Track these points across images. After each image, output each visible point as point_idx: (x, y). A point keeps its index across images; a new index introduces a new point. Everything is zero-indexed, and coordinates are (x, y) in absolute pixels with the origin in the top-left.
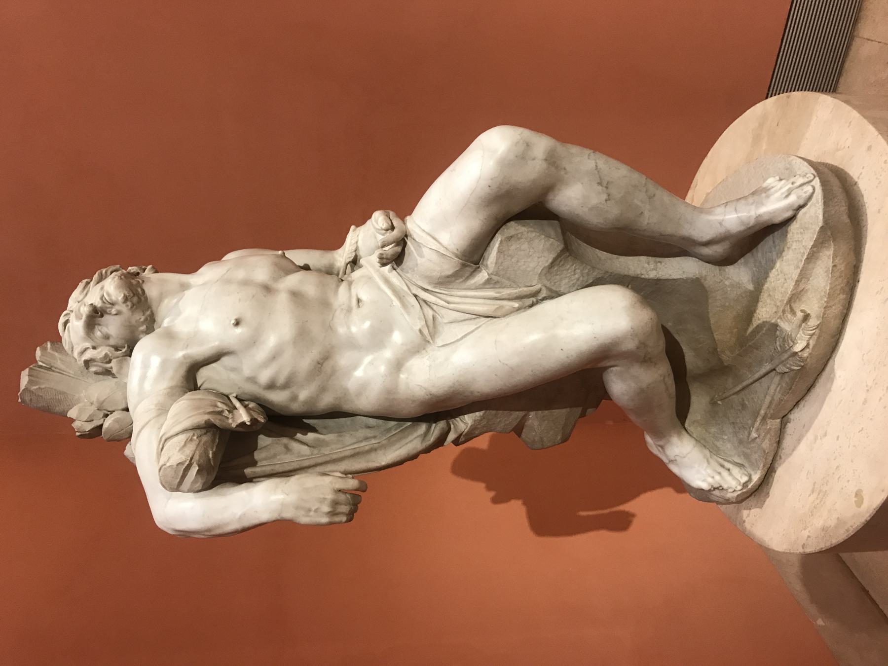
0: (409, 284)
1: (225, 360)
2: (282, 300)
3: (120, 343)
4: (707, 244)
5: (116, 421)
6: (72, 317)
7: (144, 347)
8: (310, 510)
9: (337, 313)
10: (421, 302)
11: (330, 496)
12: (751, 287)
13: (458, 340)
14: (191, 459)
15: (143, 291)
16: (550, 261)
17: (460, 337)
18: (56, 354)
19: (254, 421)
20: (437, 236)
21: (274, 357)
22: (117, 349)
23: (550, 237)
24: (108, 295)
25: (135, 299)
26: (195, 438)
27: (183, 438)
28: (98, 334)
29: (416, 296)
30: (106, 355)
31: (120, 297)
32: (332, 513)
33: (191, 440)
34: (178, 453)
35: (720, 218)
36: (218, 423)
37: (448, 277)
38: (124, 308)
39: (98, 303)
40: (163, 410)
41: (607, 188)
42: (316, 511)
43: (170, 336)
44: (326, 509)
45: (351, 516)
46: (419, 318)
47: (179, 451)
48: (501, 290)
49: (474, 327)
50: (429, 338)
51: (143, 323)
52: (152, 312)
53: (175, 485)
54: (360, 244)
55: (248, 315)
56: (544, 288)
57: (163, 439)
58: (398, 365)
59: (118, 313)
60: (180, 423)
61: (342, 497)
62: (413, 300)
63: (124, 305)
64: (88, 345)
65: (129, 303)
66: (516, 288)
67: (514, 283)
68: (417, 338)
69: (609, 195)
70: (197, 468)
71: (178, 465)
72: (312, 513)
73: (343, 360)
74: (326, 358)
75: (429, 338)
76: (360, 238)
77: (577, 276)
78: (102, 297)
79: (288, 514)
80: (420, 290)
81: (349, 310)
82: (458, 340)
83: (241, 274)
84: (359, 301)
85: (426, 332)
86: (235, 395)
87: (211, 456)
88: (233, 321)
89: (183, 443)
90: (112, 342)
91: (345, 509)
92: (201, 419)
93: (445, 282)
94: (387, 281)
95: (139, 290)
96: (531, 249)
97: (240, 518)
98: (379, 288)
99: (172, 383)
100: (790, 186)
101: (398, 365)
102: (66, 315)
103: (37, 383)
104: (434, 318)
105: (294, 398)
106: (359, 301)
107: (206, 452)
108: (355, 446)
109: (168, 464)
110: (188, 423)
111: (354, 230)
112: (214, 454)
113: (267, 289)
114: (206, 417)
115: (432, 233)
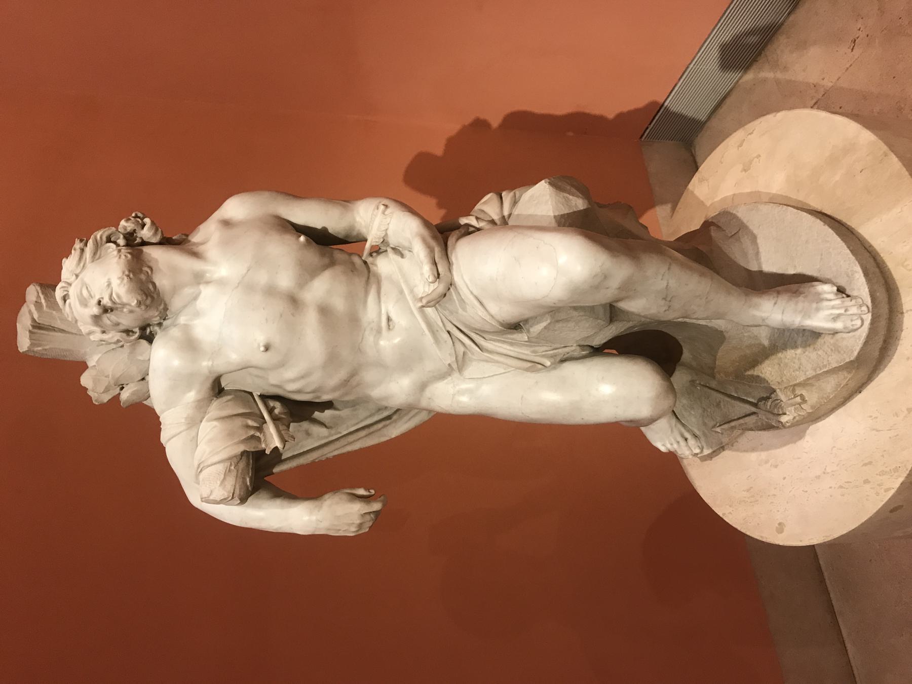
2: (311, 320)
9: (367, 333)
15: (154, 284)
23: (597, 318)
24: (119, 297)
25: (148, 302)
26: (232, 468)
29: (449, 332)
31: (134, 303)
33: (230, 471)
35: (764, 315)
40: (193, 423)
43: (190, 345)
55: (276, 340)
58: (423, 386)
60: (217, 453)
61: (368, 517)
62: (446, 336)
65: (143, 307)
69: (669, 307)
73: (369, 376)
74: (353, 374)
76: (391, 226)
80: (455, 329)
81: (379, 331)
84: (389, 319)
88: (262, 349)
90: (122, 327)
95: (151, 287)
99: (200, 397)
100: (842, 311)
103: (39, 345)
104: (464, 353)
106: (389, 319)
107: (244, 479)
110: (224, 455)
114: (242, 448)
115: (480, 297)
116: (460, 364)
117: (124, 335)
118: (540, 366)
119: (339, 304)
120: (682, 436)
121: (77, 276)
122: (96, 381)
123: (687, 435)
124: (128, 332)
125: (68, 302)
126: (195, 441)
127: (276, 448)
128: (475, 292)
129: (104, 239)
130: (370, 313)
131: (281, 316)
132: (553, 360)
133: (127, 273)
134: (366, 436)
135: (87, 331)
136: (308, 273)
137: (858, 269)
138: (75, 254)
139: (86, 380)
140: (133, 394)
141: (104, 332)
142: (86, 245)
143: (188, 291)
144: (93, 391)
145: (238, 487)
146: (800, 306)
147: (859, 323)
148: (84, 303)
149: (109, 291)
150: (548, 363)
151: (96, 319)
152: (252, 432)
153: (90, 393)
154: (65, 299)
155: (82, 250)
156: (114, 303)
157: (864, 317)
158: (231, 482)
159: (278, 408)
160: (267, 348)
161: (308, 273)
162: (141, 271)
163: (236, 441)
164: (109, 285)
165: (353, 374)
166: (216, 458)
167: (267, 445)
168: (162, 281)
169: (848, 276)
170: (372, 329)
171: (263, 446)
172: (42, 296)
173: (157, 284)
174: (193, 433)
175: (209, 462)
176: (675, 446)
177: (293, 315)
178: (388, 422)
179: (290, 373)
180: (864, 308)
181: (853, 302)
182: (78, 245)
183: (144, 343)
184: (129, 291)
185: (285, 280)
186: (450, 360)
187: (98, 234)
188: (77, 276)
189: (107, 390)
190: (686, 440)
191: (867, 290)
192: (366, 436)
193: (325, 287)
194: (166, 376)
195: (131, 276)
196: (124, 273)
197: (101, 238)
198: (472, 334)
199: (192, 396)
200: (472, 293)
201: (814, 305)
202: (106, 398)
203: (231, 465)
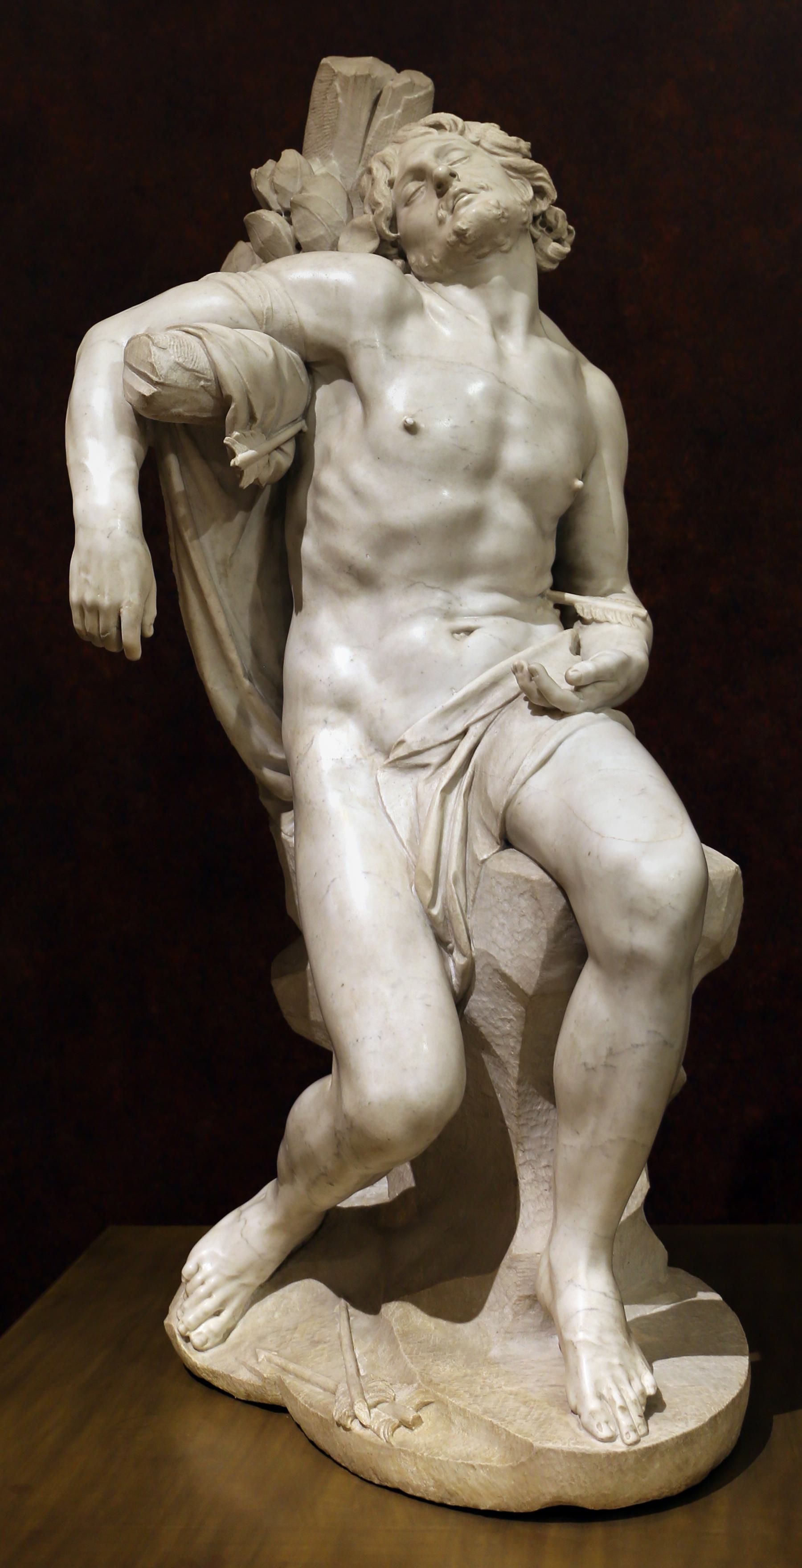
3: (401, 224)
5: (276, 232)
6: (448, 137)
9: (440, 594)
11: (105, 601)
16: (508, 971)
17: (389, 812)
18: (399, 111)
19: (238, 471)
21: (357, 493)
24: (468, 202)
26: (202, 383)
28: (412, 186)
29: (465, 732)
30: (378, 204)
31: (461, 224)
33: (199, 379)
37: (486, 790)
38: (446, 233)
40: (265, 322)
41: (606, 1065)
43: (396, 312)
46: (423, 740)
47: (178, 364)
51: (430, 261)
53: (133, 361)
54: (604, 627)
55: (424, 444)
57: (201, 333)
60: (227, 357)
62: (458, 728)
63: (451, 231)
64: (396, 173)
68: (390, 738)
70: (147, 394)
72: (83, 575)
75: (391, 758)
76: (616, 627)
79: (81, 538)
81: (448, 615)
83: (516, 418)
84: (469, 631)
87: (174, 411)
88: (410, 421)
90: (403, 212)
92: (233, 388)
94: (494, 683)
95: (486, 250)
98: (488, 667)
99: (309, 329)
101: (346, 704)
103: (344, 89)
104: (425, 766)
106: (469, 631)
109: (154, 349)
110: (225, 369)
112: (179, 416)
113: (485, 470)
115: (554, 758)
117: (389, 213)
118: (429, 894)
119: (489, 544)
120: (223, 1304)
121: (477, 144)
122: (295, 172)
123: (225, 1315)
124: (393, 222)
125: (432, 130)
127: (234, 455)
130: (475, 600)
131: (464, 449)
132: (440, 919)
135: (389, 159)
136: (529, 491)
137: (692, 1425)
138: (512, 141)
142: (525, 157)
146: (609, 1338)
147: (605, 1433)
149: (474, 189)
150: (435, 911)
151: (419, 173)
153: (270, 164)
154: (439, 126)
156: (456, 196)
157: (618, 1442)
158: (179, 378)
159: (285, 461)
160: (411, 429)
161: (529, 491)
162: (508, 235)
163: (248, 387)
166: (217, 355)
169: (674, 1416)
170: (450, 603)
172: (422, 93)
174: (244, 321)
175: (210, 345)
180: (633, 1437)
181: (637, 1420)
182: (524, 145)
183: (374, 244)
184: (479, 216)
185: (517, 456)
186: (413, 740)
187: (544, 174)
188: (477, 144)
189: (277, 190)
191: (663, 1439)
193: (509, 521)
194: (323, 280)
195: (503, 221)
196: (506, 209)
197: (540, 179)
198: (468, 775)
200: (560, 743)
201: (616, 1361)
202: (263, 187)
203: (207, 380)
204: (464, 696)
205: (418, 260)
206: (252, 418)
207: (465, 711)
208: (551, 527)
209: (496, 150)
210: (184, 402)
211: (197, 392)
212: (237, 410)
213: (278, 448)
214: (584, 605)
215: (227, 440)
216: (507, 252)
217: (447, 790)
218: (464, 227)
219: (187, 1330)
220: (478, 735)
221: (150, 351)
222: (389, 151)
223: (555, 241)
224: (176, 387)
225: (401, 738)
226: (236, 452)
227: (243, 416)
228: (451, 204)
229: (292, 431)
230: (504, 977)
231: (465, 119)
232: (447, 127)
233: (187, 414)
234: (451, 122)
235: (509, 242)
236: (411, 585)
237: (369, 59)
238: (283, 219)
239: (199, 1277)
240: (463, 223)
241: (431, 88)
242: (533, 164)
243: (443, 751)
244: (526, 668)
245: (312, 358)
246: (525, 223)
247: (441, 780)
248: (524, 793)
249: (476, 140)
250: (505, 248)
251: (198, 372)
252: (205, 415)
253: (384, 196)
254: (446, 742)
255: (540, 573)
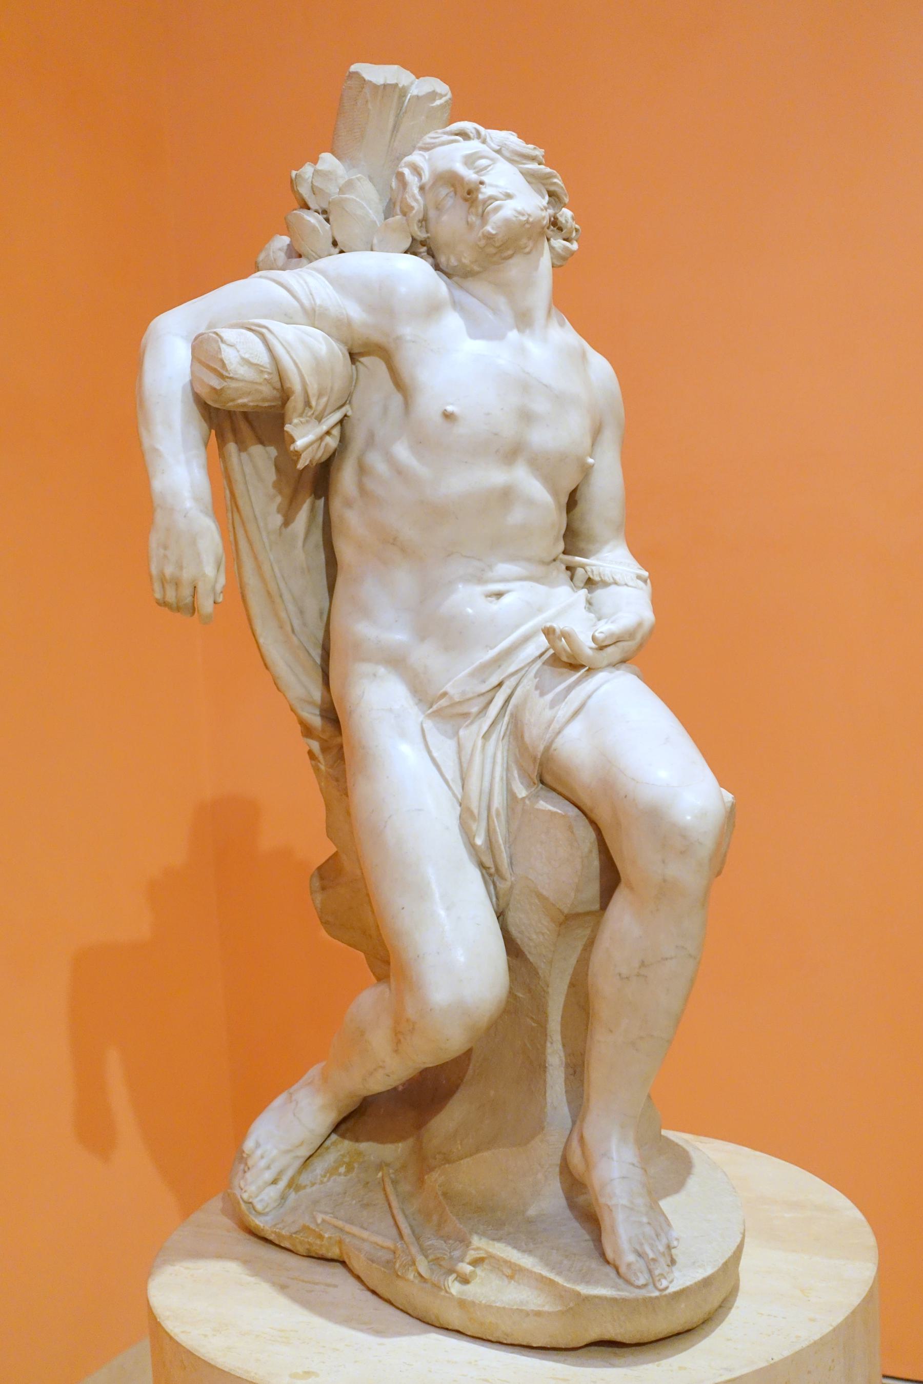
0: (520, 675)
1: (398, 398)
4: (582, 1139)
6: (473, 146)
7: (415, 271)
8: (165, 547)
10: (491, 694)
12: (532, 1212)
13: (429, 752)
14: (231, 378)
15: (510, 257)
16: (545, 893)
17: (435, 754)
19: (298, 454)
20: (581, 717)
22: (424, 221)
24: (497, 209)
25: (492, 250)
26: (266, 376)
27: (263, 358)
29: (500, 685)
31: (489, 228)
32: (163, 581)
33: (262, 372)
34: (241, 352)
36: (290, 405)
37: (522, 737)
39: (486, 192)
42: (165, 556)
43: (431, 310)
44: (169, 571)
45: (164, 603)
46: (463, 693)
48: (503, 818)
49: (449, 777)
50: (435, 707)
52: (478, 273)
56: (509, 883)
57: (264, 330)
58: (396, 661)
59: (470, 226)
61: (186, 592)
62: (494, 681)
64: (426, 176)
65: (482, 243)
66: (505, 843)
67: (511, 842)
70: (218, 387)
71: (222, 361)
72: (162, 551)
74: (405, 550)
75: (435, 707)
77: (534, 937)
78: (493, 198)
79: (160, 518)
80: (509, 691)
82: (429, 752)
84: (499, 595)
85: (443, 702)
86: (349, 414)
87: (240, 401)
88: (450, 408)
89: (255, 361)
90: (432, 214)
91: (171, 596)
93: (516, 732)
95: (510, 252)
96: (557, 865)
97: (156, 450)
102: (478, 133)
104: (466, 715)
105: (348, 504)
106: (499, 595)
108: (287, 596)
109: (223, 346)
111: (639, 577)
112: (244, 405)
114: (297, 387)
115: (585, 710)
116: (447, 712)
119: (517, 516)
120: (280, 1173)
124: (424, 221)
126: (289, 319)
128: (591, 703)
129: (552, 188)
131: (496, 434)
133: (531, 220)
134: (269, 593)
138: (529, 149)
139: (327, 161)
140: (314, 229)
141: (422, 188)
143: (502, 302)
144: (316, 172)
145: (240, 384)
148: (470, 160)
152: (313, 403)
154: (464, 135)
155: (533, 159)
159: (332, 442)
160: (448, 416)
162: (529, 239)
164: (509, 196)
165: (405, 550)
167: (296, 426)
168: (514, 269)
171: (296, 421)
173: (511, 261)
176: (263, 1163)
177: (497, 451)
178: (289, 629)
179: (402, 452)
182: (539, 153)
183: (407, 244)
184: (507, 222)
188: (498, 152)
189: (314, 190)
190: (275, 1182)
192: (269, 593)
195: (527, 226)
197: (555, 184)
199: (355, 312)
203: (269, 373)
204: (499, 654)
205: (448, 260)
206: (308, 404)
207: (500, 666)
208: (564, 499)
209: (516, 158)
210: (249, 394)
211: (260, 384)
212: (297, 401)
213: (328, 433)
214: (594, 568)
215: (288, 428)
216: (529, 253)
217: (486, 736)
218: (494, 232)
219: (250, 1197)
220: (512, 688)
221: (220, 348)
222: (416, 157)
223: (564, 240)
224: (242, 381)
225: (443, 690)
226: (296, 438)
227: (300, 405)
228: (480, 210)
229: (337, 416)
230: (539, 896)
231: (487, 127)
232: (471, 135)
233: (252, 404)
234: (474, 131)
235: (531, 244)
236: (449, 555)
237: (395, 68)
238: (321, 217)
239: (259, 1152)
240: (493, 228)
241: (449, 95)
242: (548, 170)
243: (483, 701)
244: (558, 631)
245: (356, 351)
246: (543, 228)
247: (480, 728)
248: (559, 741)
249: (498, 148)
250: (527, 250)
251: (262, 366)
252: (266, 404)
253: (415, 200)
254: (483, 694)
255: (556, 540)
